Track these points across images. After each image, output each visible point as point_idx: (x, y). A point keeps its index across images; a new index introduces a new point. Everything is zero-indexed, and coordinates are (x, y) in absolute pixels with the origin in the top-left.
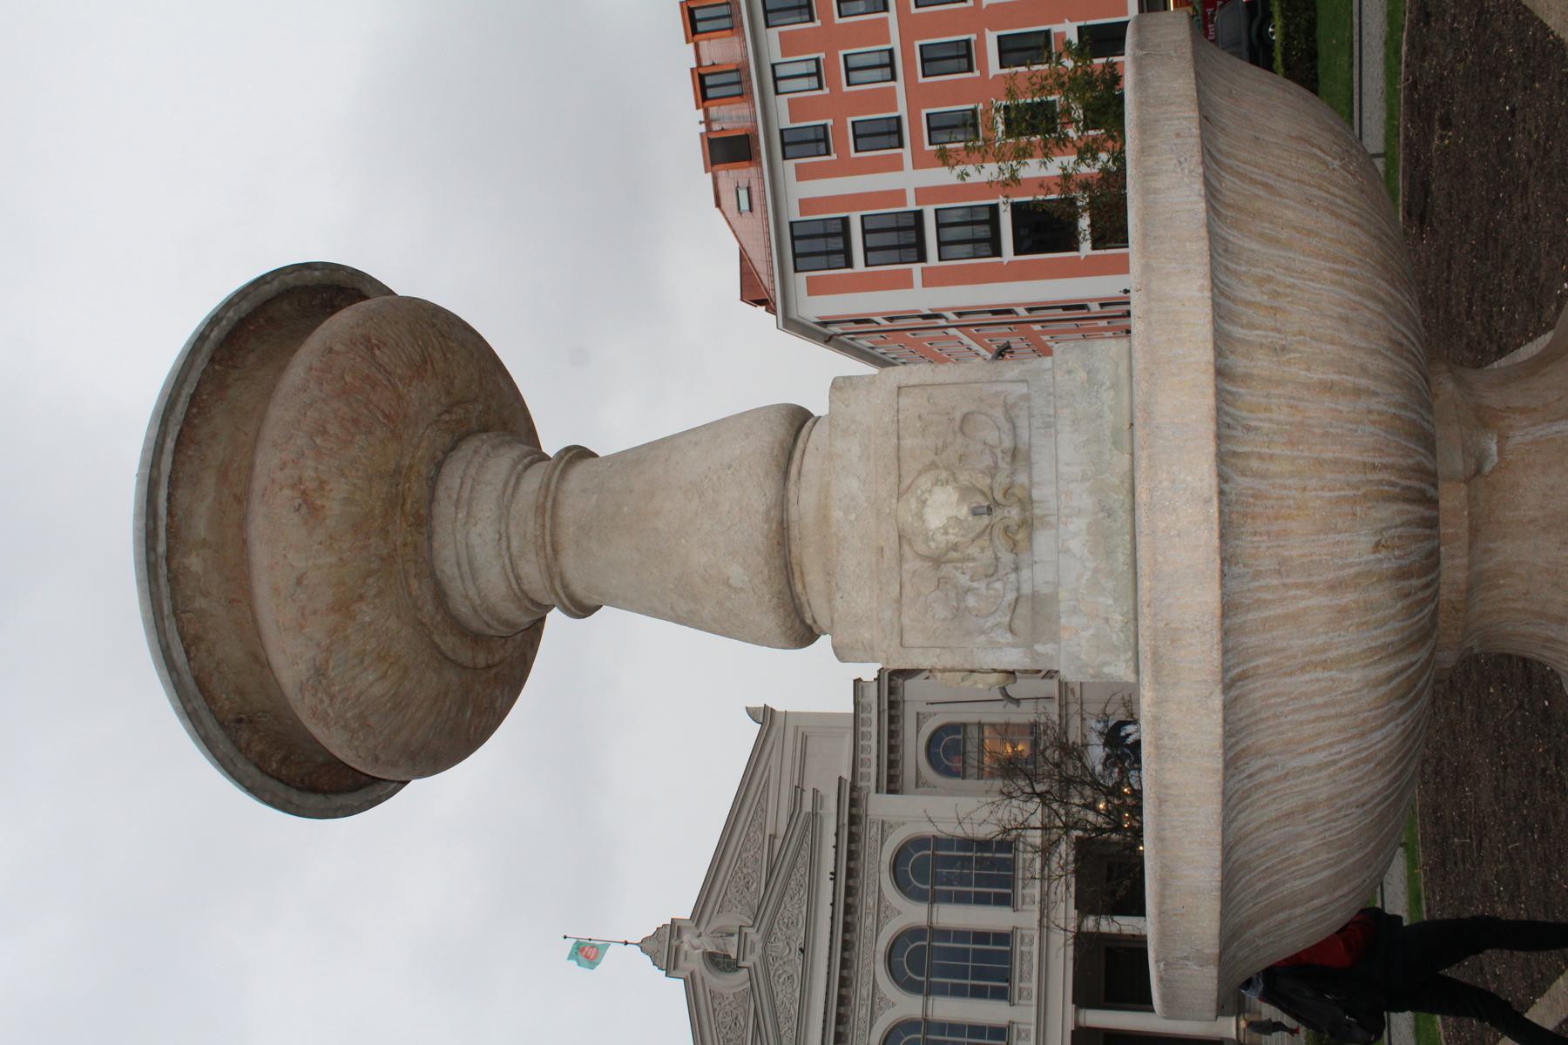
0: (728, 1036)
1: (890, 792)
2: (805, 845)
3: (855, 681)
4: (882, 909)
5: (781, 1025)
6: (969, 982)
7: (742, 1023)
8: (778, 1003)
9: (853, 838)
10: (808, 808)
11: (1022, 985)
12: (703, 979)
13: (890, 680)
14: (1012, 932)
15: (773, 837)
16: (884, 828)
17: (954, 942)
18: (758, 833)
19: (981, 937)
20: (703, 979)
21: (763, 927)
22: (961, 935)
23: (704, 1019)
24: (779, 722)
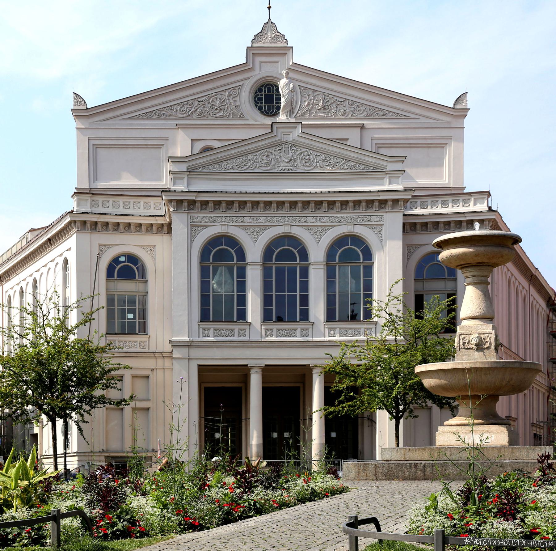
0: (207, 104)
1: (404, 224)
2: (363, 167)
3: (488, 192)
4: (320, 229)
5: (234, 161)
6: (274, 294)
7: (218, 115)
8: (250, 157)
9: (370, 203)
10: (391, 167)
11: (275, 331)
12: (248, 78)
13: (489, 220)
14: (309, 322)
15: (362, 127)
16: (378, 227)
17: (300, 281)
18: (365, 113)
19: (305, 300)
20: (248, 78)
21: (302, 140)
22: (305, 286)
23: (218, 83)
24: (455, 123)
